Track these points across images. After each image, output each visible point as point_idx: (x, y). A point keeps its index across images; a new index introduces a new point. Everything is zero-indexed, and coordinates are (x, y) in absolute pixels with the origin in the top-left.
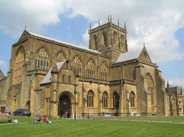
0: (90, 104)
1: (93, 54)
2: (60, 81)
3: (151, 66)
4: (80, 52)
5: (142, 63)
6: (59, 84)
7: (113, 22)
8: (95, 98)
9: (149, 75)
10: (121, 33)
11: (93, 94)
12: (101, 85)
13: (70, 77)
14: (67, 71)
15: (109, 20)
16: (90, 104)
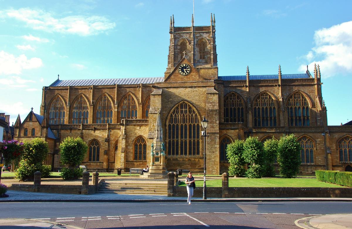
0: (94, 157)
1: (131, 87)
2: (22, 135)
3: (195, 87)
4: (109, 90)
5: (167, 88)
6: (20, 139)
7: (176, 25)
8: (100, 149)
9: (187, 105)
10: (201, 36)
11: (99, 145)
12: (112, 132)
13: (33, 130)
14: (31, 123)
15: (171, 24)
16: (94, 157)
